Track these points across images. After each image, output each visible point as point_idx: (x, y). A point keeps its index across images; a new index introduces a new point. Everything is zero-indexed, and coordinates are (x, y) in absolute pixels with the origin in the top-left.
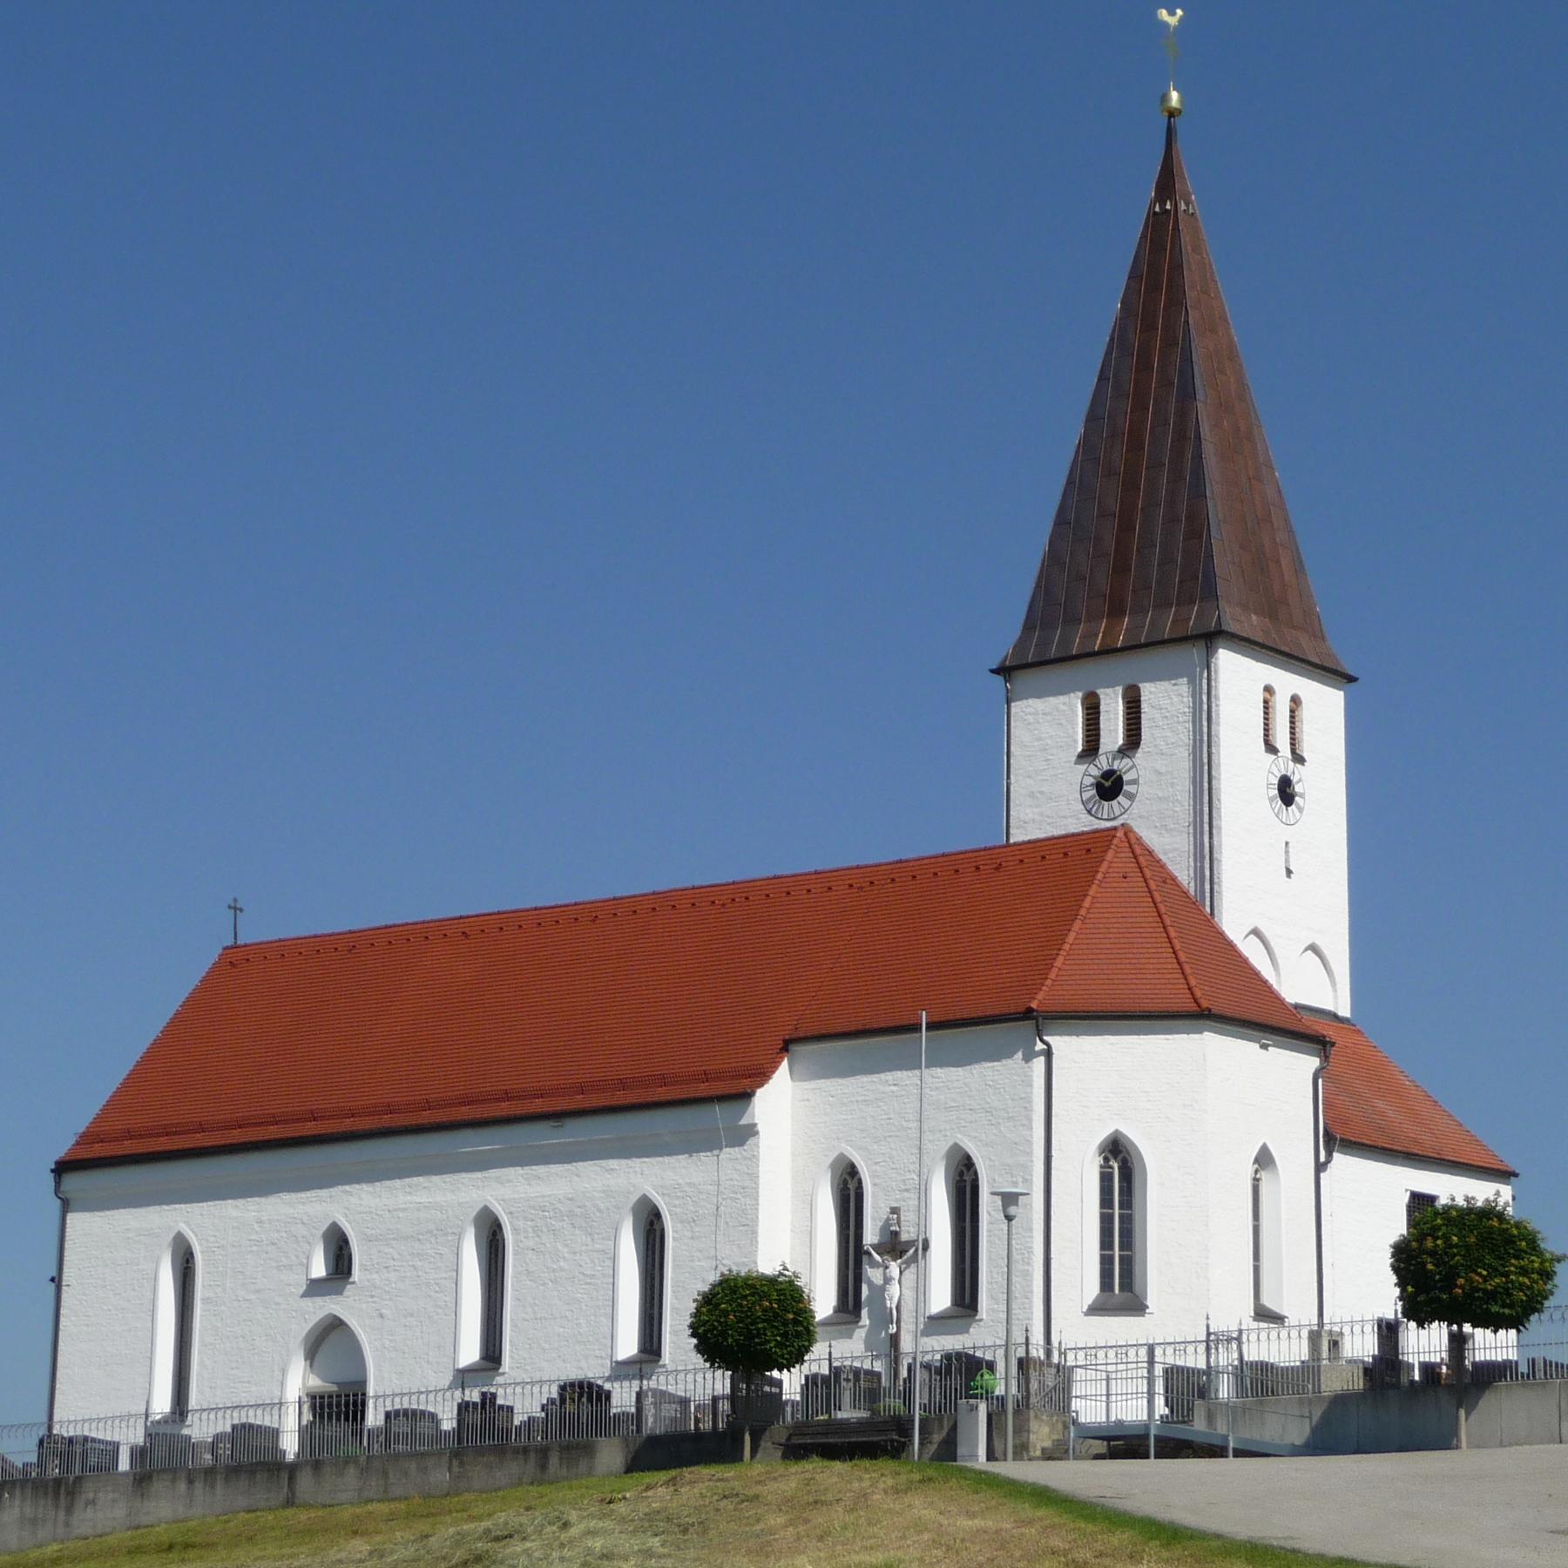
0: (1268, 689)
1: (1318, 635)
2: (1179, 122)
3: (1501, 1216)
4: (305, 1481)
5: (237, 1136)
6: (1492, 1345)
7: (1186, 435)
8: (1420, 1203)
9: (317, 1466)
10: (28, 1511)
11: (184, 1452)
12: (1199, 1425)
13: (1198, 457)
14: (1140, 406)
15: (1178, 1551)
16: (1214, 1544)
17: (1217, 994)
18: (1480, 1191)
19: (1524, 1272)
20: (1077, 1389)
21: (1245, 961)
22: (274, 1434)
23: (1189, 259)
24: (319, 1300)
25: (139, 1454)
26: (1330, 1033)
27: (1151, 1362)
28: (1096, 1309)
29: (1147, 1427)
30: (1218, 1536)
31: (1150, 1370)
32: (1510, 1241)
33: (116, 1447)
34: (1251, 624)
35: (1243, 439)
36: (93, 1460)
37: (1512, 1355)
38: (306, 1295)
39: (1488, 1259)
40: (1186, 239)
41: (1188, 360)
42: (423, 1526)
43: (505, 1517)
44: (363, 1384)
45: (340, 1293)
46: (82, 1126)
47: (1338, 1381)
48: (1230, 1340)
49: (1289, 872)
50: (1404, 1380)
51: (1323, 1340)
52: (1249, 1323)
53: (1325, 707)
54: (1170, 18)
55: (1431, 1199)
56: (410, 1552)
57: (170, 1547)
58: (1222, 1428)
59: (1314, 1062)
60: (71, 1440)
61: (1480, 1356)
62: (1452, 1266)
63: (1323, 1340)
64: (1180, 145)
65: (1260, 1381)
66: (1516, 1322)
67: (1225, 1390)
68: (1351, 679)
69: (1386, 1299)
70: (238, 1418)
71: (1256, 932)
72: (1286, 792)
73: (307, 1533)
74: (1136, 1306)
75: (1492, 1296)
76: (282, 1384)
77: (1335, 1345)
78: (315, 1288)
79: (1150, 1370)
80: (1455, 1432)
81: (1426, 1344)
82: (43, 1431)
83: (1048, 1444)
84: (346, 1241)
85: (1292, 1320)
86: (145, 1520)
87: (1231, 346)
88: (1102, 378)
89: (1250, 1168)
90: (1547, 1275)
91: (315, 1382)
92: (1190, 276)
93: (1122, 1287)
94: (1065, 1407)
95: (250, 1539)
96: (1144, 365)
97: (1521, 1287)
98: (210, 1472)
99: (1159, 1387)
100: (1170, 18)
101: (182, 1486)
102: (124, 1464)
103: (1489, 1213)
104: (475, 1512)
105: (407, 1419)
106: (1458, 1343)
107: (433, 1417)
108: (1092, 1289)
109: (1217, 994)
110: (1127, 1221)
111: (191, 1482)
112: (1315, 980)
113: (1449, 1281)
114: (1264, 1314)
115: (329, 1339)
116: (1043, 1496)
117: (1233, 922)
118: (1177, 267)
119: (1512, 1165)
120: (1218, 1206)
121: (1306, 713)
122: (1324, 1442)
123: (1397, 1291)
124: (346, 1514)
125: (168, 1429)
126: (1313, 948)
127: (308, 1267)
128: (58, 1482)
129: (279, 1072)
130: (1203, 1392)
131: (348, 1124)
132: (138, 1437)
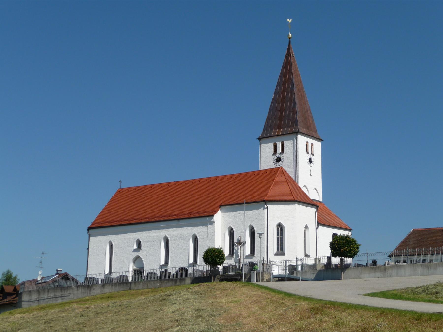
0: (307, 142)
1: (316, 132)
2: (291, 39)
3: (349, 237)
4: (133, 285)
5: (120, 223)
6: (348, 261)
7: (292, 96)
8: (335, 235)
9: (135, 283)
10: (83, 291)
11: (111, 280)
12: (295, 275)
13: (294, 100)
14: (284, 91)
15: (291, 298)
16: (298, 297)
17: (299, 198)
18: (346, 233)
19: (353, 247)
20: (273, 269)
21: (303, 191)
22: (127, 277)
23: (293, 64)
24: (135, 253)
25: (103, 281)
26: (318, 204)
27: (286, 264)
28: (276, 254)
29: (285, 275)
30: (298, 295)
31: (286, 265)
32: (351, 242)
33: (99, 279)
34: (304, 130)
35: (302, 97)
36: (94, 282)
37: (351, 263)
38: (133, 252)
39: (347, 245)
40: (292, 61)
41: (293, 83)
42: (154, 293)
43: (169, 292)
44: (143, 268)
45: (139, 251)
46: (92, 221)
47: (319, 267)
48: (300, 260)
49: (311, 175)
50: (332, 267)
51: (317, 260)
52: (304, 257)
53: (317, 145)
54: (289, 21)
55: (337, 234)
56: (152, 298)
57: (108, 297)
58: (299, 276)
59: (315, 210)
60: (90, 278)
61: (345, 263)
62: (341, 246)
63: (317, 260)
64: (291, 44)
65: (306, 267)
66: (352, 257)
67: (299, 269)
68: (322, 140)
69: (328, 252)
70: (121, 274)
71: (305, 186)
72: (310, 161)
73: (133, 295)
74: (283, 254)
75: (348, 252)
76: (129, 268)
77: (319, 261)
78: (135, 250)
79: (286, 265)
80: (341, 277)
81: (336, 261)
82: (85, 276)
83: (267, 279)
84: (140, 242)
85: (311, 256)
86: (104, 292)
87: (300, 80)
88: (277, 86)
89: (304, 229)
90: (358, 248)
91: (135, 267)
92: (293, 67)
93: (281, 250)
94: (270, 272)
95: (123, 296)
96: (285, 84)
97: (353, 250)
98: (116, 284)
99: (287, 268)
100: (289, 21)
101: (111, 286)
102: (100, 282)
103: (347, 237)
104: (164, 291)
105: (152, 275)
106: (342, 260)
107: (156, 274)
108: (275, 251)
109: (299, 198)
110: (282, 238)
111: (112, 286)
112: (316, 195)
113: (340, 249)
114: (306, 255)
115: (137, 260)
116: (266, 288)
117: (301, 184)
118: (291, 66)
119: (351, 228)
120: (297, 236)
121: (314, 146)
122: (317, 278)
123: (330, 251)
124: (140, 291)
125: (108, 276)
126: (315, 189)
127: (133, 247)
128: (88, 285)
129: (128, 211)
130: (295, 269)
131: (141, 221)
132: (102, 277)
